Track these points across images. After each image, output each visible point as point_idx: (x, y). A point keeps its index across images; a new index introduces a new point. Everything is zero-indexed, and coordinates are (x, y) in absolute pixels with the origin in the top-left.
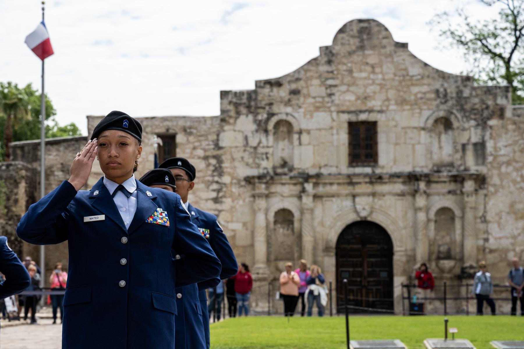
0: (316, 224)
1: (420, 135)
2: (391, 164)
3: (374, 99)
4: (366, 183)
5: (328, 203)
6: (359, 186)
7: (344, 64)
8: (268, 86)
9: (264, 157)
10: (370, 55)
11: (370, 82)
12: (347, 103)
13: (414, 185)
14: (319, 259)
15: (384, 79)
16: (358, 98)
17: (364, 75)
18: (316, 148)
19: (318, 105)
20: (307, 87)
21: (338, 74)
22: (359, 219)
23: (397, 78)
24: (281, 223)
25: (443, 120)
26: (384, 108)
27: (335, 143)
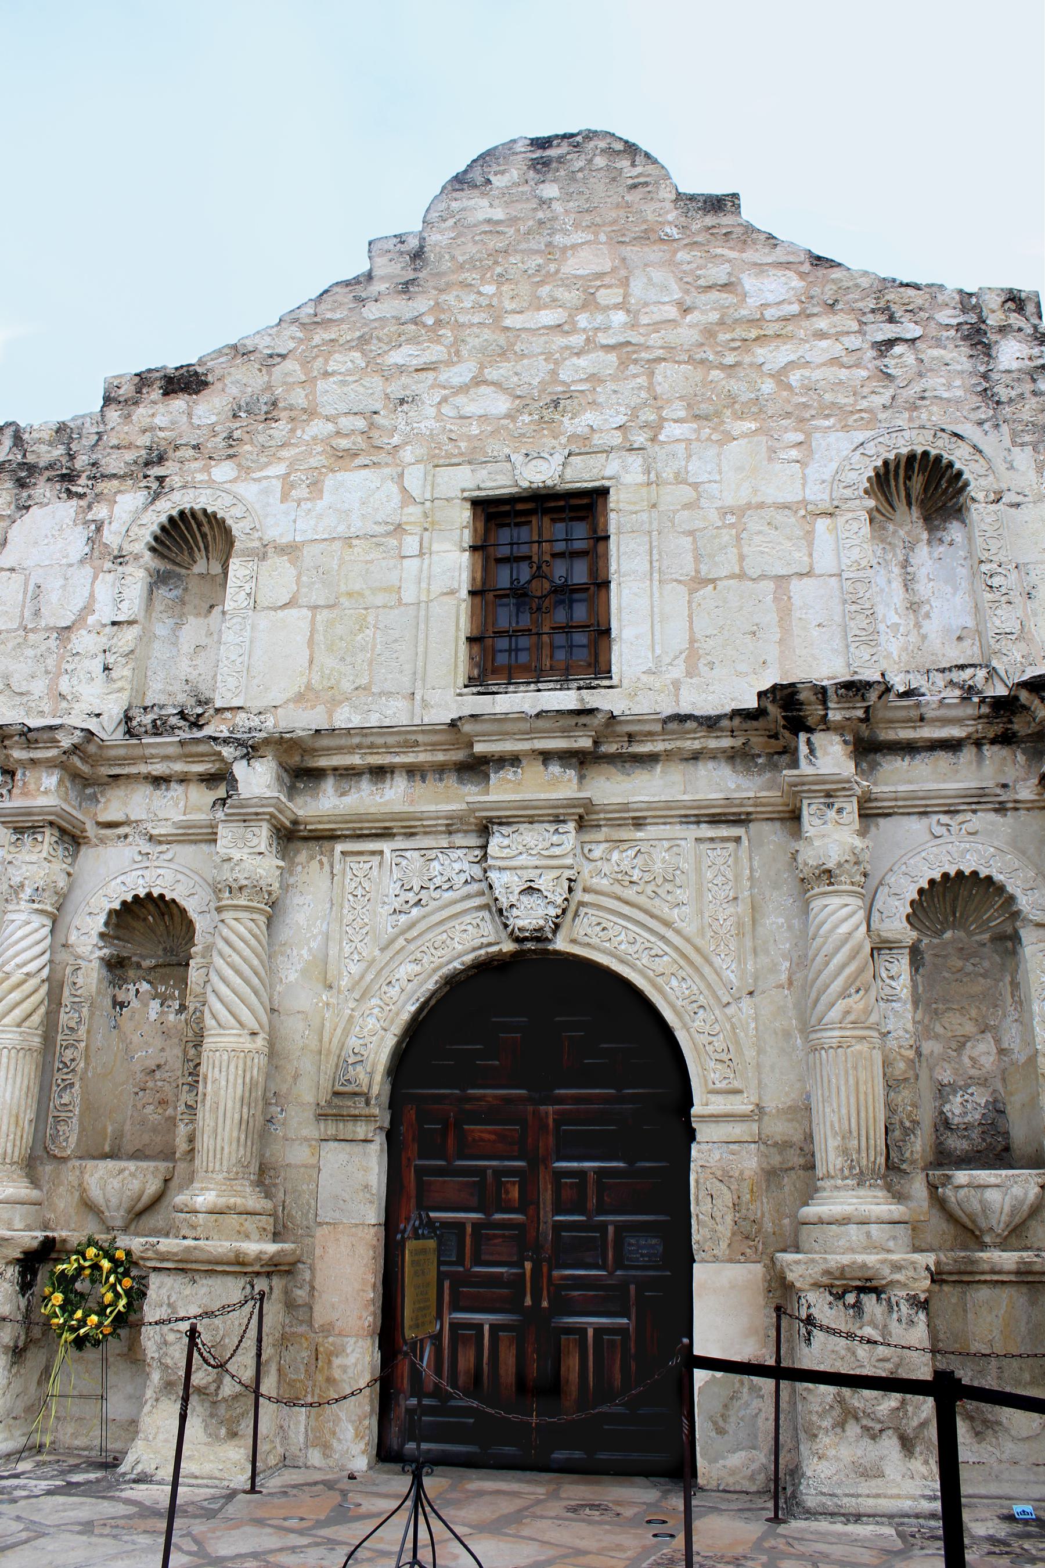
0: (291, 973)
1: (809, 536)
2: (678, 671)
3: (593, 403)
4: (546, 757)
5: (359, 866)
6: (508, 774)
7: (465, 285)
8: (156, 394)
9: (97, 666)
10: (574, 247)
11: (577, 340)
12: (475, 430)
13: (790, 754)
14: (298, 1155)
15: (634, 326)
16: (523, 402)
17: (548, 317)
18: (322, 616)
19: (344, 443)
20: (309, 382)
21: (438, 322)
22: (508, 947)
23: (689, 318)
24: (151, 975)
25: (917, 483)
26: (639, 439)
27: (408, 596)
